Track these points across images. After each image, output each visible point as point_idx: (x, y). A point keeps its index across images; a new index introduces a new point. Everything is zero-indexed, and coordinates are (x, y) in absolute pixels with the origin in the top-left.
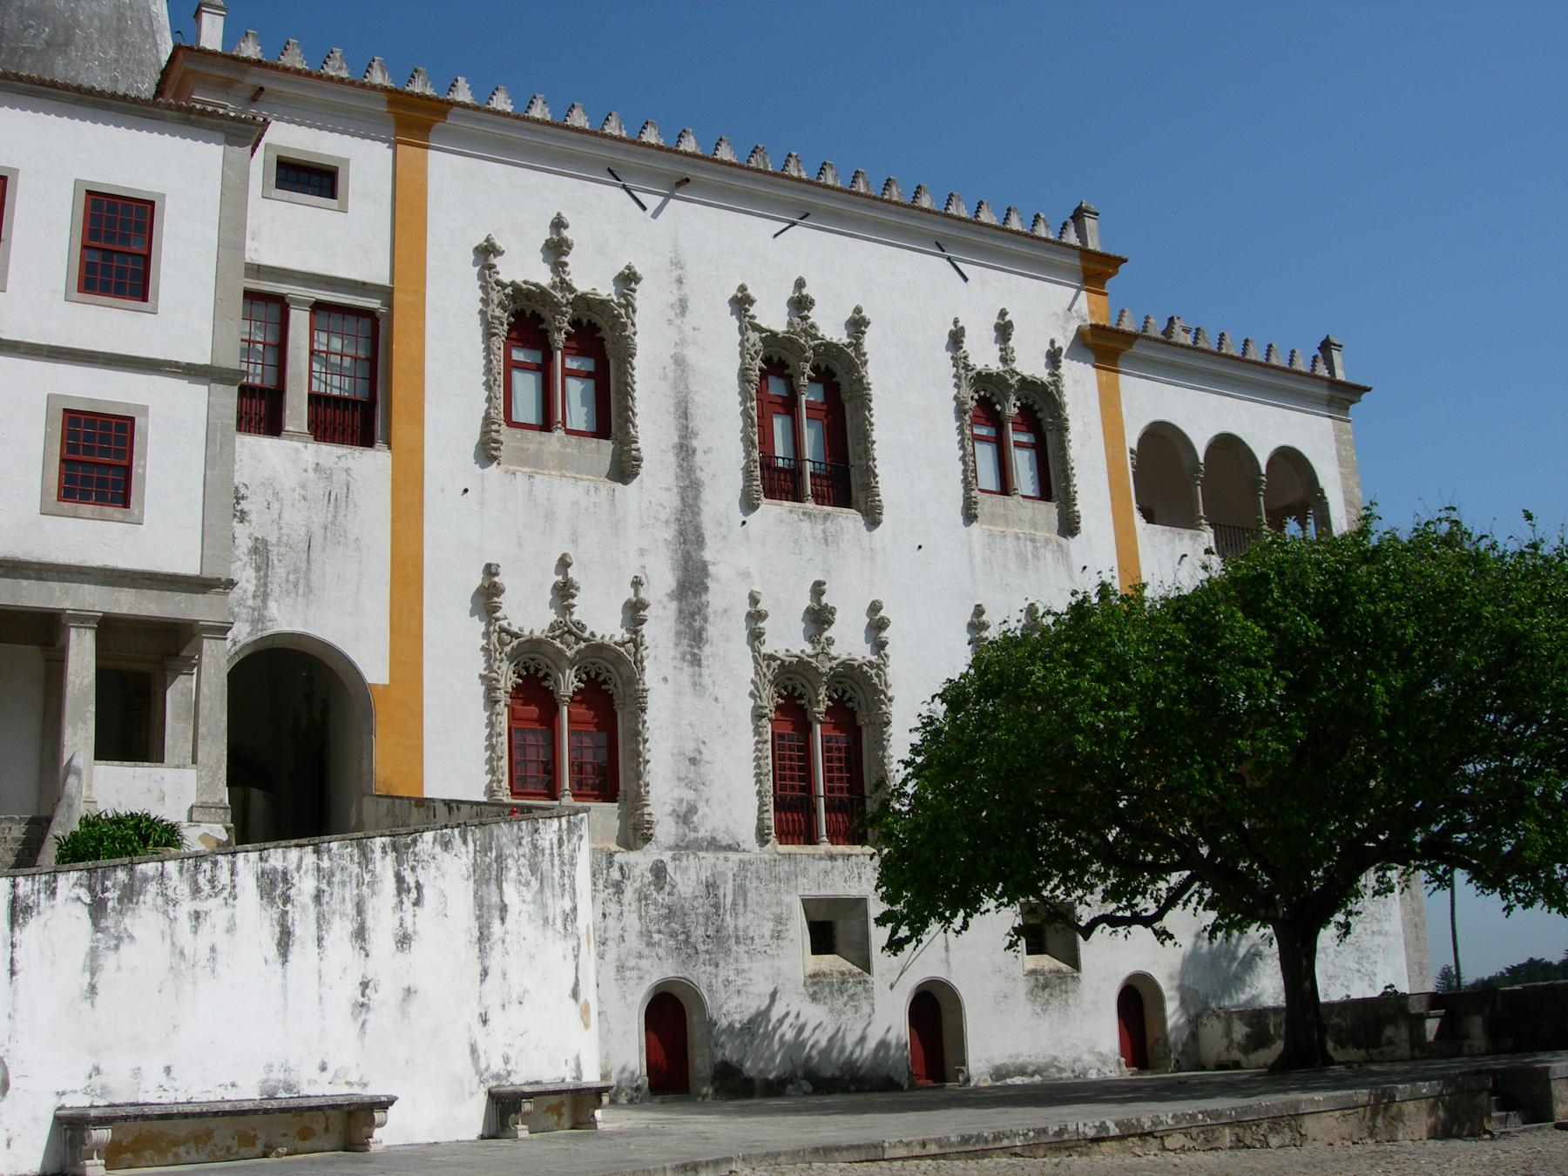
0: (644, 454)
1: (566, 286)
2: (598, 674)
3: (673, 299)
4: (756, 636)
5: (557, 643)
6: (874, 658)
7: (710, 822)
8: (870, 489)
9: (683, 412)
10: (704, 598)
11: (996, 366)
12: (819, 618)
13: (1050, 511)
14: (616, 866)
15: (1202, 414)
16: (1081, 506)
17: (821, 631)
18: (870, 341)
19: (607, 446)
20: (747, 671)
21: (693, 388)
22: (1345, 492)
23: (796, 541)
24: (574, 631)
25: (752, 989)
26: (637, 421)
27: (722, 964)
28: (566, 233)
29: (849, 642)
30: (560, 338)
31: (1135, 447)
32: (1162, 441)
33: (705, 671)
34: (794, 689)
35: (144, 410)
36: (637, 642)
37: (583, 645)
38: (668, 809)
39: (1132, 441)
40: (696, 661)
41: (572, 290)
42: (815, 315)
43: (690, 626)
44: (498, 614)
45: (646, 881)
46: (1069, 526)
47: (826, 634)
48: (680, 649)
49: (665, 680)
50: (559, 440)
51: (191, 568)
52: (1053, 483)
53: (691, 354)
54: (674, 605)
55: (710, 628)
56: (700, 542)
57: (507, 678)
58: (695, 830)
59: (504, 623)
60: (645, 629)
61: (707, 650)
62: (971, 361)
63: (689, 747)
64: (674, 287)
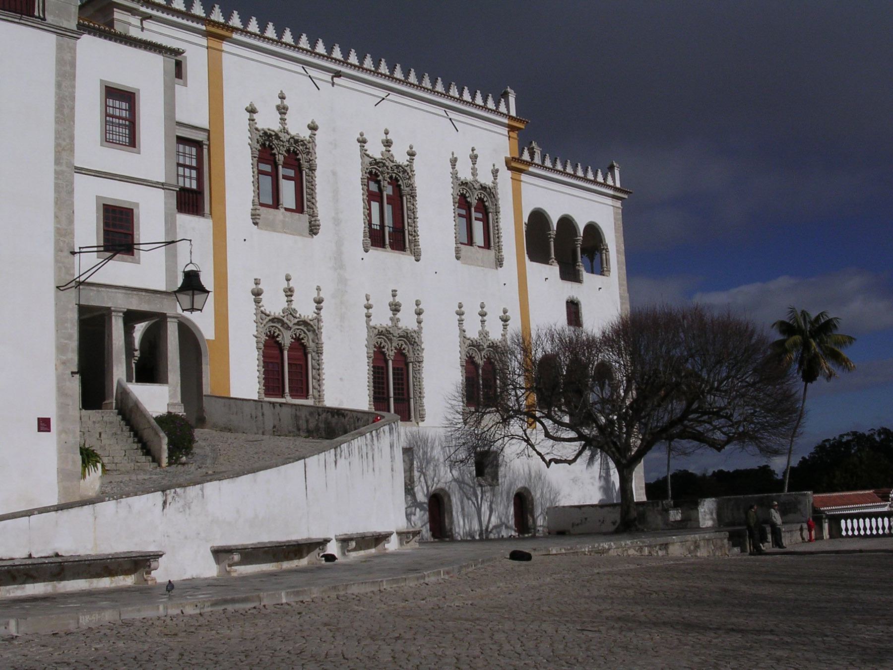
4: (368, 316)
5: (285, 319)
6: (416, 329)
8: (415, 243)
11: (470, 178)
12: (395, 308)
13: (491, 253)
16: (504, 253)
19: (305, 218)
20: (363, 334)
24: (292, 313)
28: (286, 102)
29: (407, 321)
30: (280, 159)
32: (538, 218)
35: (137, 205)
37: (296, 320)
39: (525, 219)
41: (288, 133)
46: (499, 262)
47: (397, 316)
51: (163, 289)
57: (264, 338)
60: (322, 312)
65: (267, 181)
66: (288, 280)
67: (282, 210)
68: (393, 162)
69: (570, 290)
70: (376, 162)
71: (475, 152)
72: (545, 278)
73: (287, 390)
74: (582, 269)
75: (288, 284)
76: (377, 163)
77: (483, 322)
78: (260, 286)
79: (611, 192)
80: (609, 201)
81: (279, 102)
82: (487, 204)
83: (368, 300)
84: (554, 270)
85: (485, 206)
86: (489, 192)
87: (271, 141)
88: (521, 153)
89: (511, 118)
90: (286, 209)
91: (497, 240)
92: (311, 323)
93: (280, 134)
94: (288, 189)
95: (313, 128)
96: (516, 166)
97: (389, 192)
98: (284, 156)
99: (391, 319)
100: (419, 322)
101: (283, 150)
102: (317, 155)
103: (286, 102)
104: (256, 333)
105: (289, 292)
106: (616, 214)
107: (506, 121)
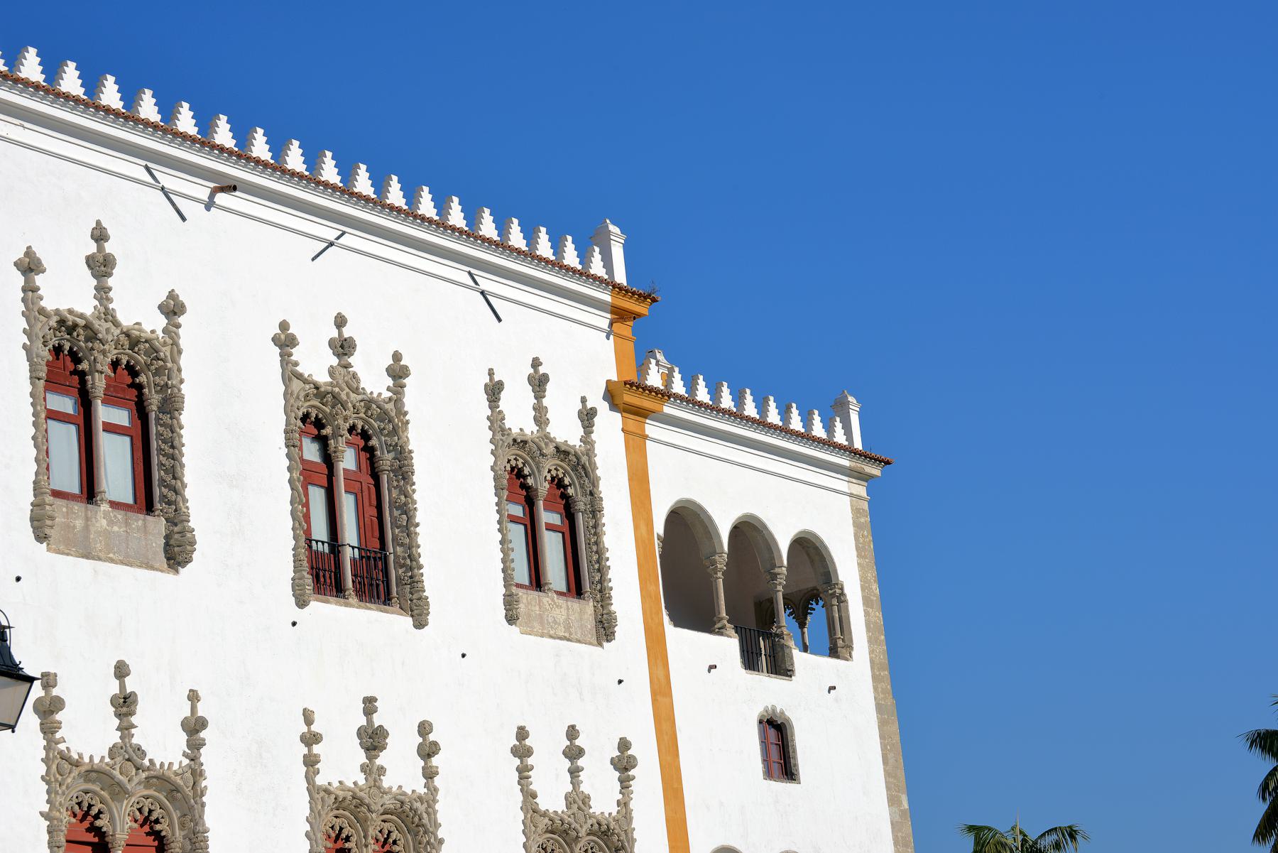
0: (198, 535)
1: (108, 315)
4: (311, 762)
5: (116, 773)
6: (422, 790)
8: (414, 583)
11: (530, 428)
12: (373, 740)
13: (585, 610)
17: (371, 758)
19: (157, 526)
20: (301, 805)
22: (863, 589)
26: (188, 493)
28: (109, 247)
29: (400, 770)
30: (98, 384)
31: (661, 532)
32: (686, 523)
36: (196, 773)
39: (659, 528)
41: (116, 324)
44: (58, 736)
46: (605, 629)
47: (378, 762)
50: (106, 514)
52: (583, 578)
59: (62, 747)
65: (65, 439)
67: (105, 507)
69: (767, 691)
70: (319, 392)
71: (542, 370)
72: (707, 659)
74: (792, 644)
75: (122, 686)
77: (574, 772)
78: (55, 692)
79: (845, 462)
80: (841, 483)
81: (92, 248)
82: (570, 491)
84: (727, 646)
85: (565, 496)
86: (578, 464)
87: (73, 341)
88: (642, 369)
89: (617, 288)
90: (115, 505)
92: (178, 780)
94: (116, 458)
95: (172, 309)
96: (631, 399)
97: (351, 464)
98: (107, 377)
99: (364, 768)
100: (429, 774)
101: (104, 365)
102: (184, 375)
103: (109, 247)
104: (46, 808)
105: (125, 704)
106: (856, 512)
107: (606, 297)
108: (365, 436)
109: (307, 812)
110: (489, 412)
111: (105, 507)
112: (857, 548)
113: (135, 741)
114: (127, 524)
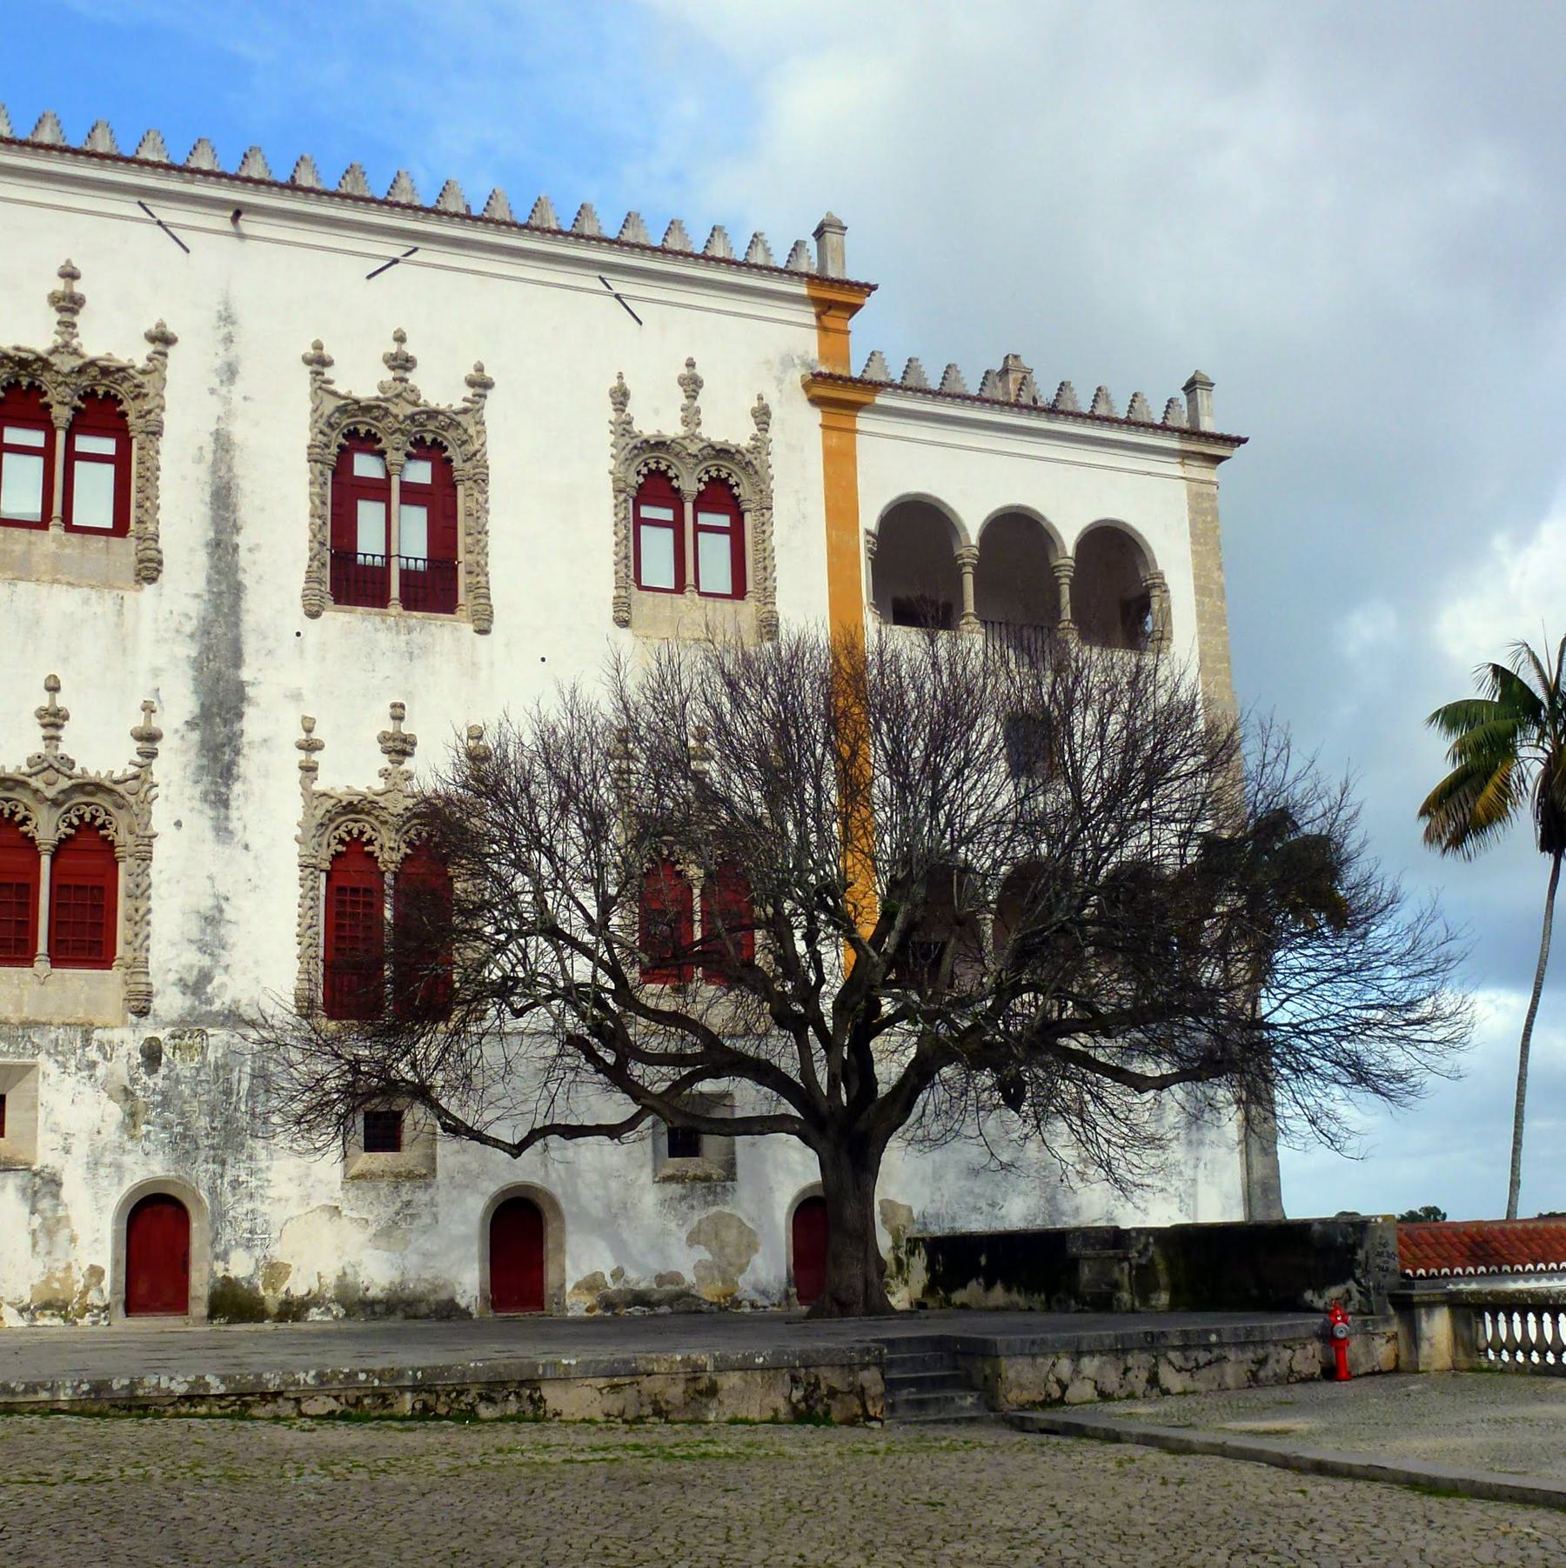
2: (94, 818)
3: (218, 363)
4: (309, 769)
5: (35, 782)
7: (231, 989)
8: (481, 593)
9: (223, 499)
10: (237, 727)
14: (95, 1044)
15: (976, 479)
18: (494, 407)
21: (238, 470)
22: (1196, 577)
23: (369, 656)
25: (271, 1193)
27: (230, 1160)
30: (61, 415)
33: (233, 814)
34: (362, 833)
38: (173, 977)
40: (222, 802)
41: (82, 357)
42: (413, 378)
43: (215, 759)
45: (134, 1062)
48: (200, 788)
49: (178, 824)
50: (55, 539)
53: (239, 431)
54: (195, 736)
55: (241, 761)
56: (237, 659)
58: (210, 1002)
60: (157, 766)
61: (237, 788)
62: (636, 428)
63: (207, 903)
64: (221, 350)
66: (53, 687)
68: (415, 404)
73: (42, 946)
76: (367, 409)
81: (60, 285)
83: (309, 731)
85: (736, 498)
87: (32, 376)
91: (761, 574)
92: (119, 788)
93: (53, 359)
98: (75, 409)
99: (384, 774)
105: (53, 720)
108: (438, 446)
109: (300, 817)
110: (613, 416)
111: (55, 530)
112: (1192, 535)
113: (63, 749)
114: (83, 546)
